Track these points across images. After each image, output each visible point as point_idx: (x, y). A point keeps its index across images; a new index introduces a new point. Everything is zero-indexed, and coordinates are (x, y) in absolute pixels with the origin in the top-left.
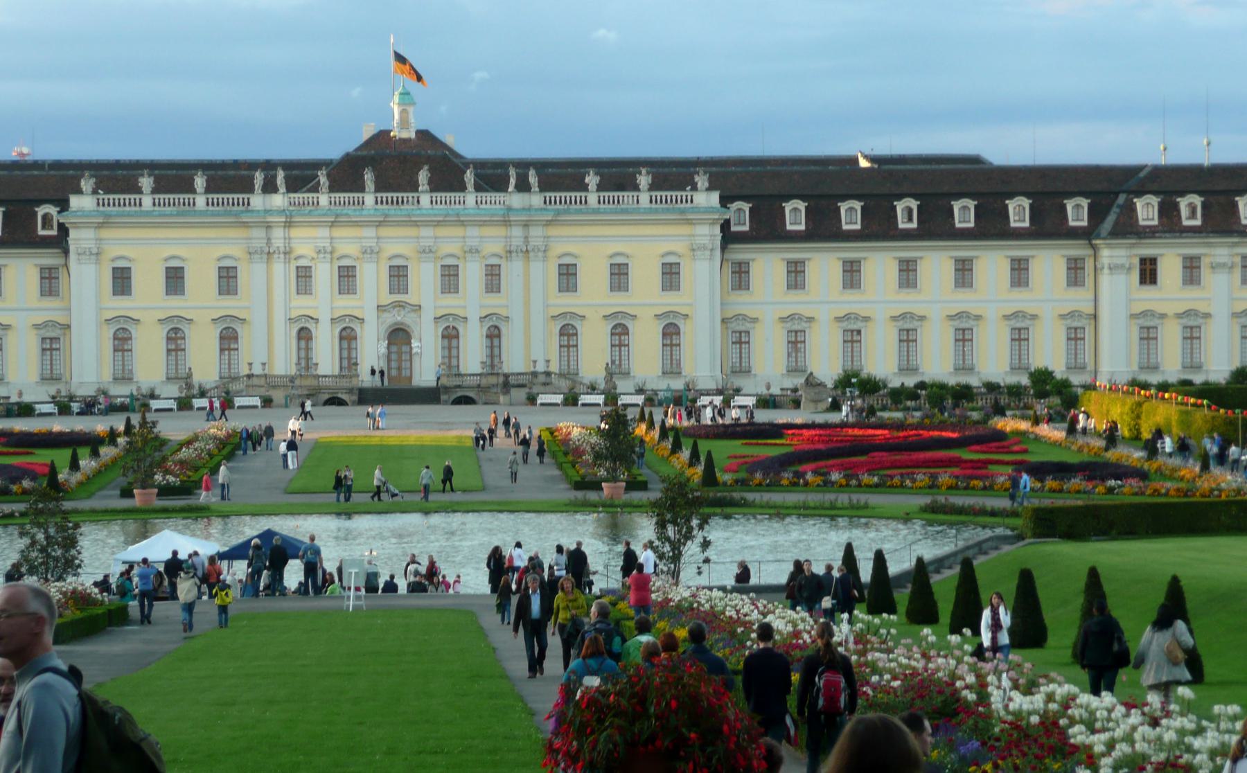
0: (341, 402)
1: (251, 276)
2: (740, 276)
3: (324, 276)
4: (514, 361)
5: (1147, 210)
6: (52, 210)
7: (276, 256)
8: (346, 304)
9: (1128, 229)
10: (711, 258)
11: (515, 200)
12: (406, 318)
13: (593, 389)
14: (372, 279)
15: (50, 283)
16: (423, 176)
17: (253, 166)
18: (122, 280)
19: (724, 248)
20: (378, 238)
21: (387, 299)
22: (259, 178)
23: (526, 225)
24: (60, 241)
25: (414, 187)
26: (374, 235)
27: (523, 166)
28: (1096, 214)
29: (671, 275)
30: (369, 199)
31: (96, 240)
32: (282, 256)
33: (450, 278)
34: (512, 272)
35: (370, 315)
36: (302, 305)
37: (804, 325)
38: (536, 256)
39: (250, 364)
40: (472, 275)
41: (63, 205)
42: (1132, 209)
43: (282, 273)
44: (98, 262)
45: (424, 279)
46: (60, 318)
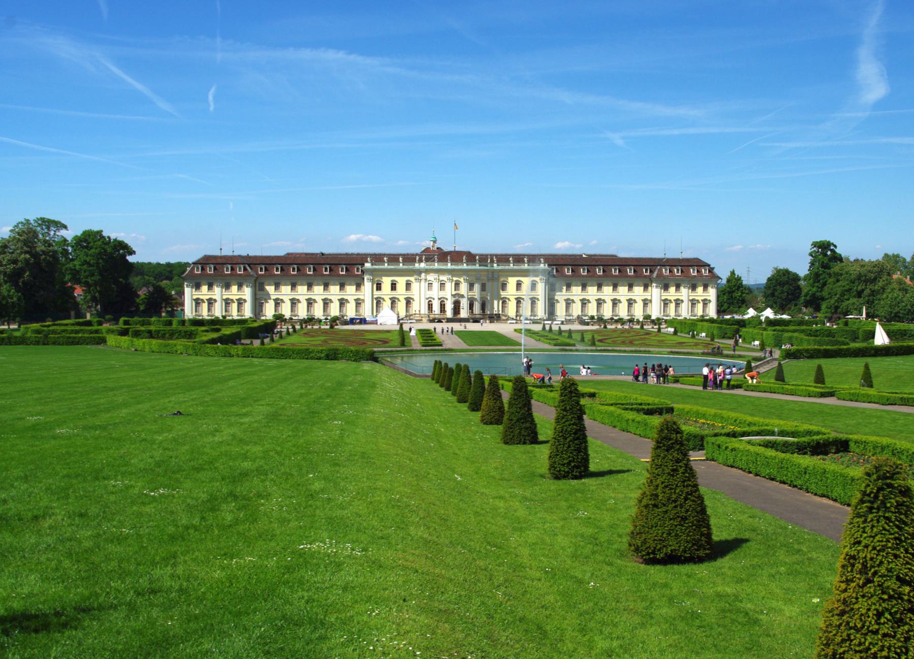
0: (442, 322)
1: (415, 286)
3: (436, 285)
5: (665, 272)
6: (360, 267)
8: (442, 294)
13: (513, 319)
14: (450, 287)
18: (379, 287)
21: (454, 293)
22: (417, 258)
25: (462, 261)
29: (533, 286)
30: (449, 264)
35: (449, 296)
36: (429, 294)
41: (363, 265)
42: (660, 270)
43: (424, 285)
45: (464, 289)
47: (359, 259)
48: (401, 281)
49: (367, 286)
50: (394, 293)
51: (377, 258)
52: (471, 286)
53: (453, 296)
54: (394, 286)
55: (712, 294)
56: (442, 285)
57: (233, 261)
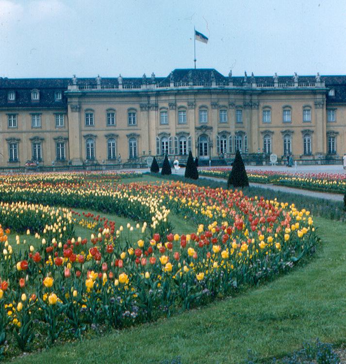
1: (141, 116)
7: (152, 108)
10: (323, 108)
12: (207, 133)
19: (327, 105)
20: (195, 99)
23: (251, 95)
26: (193, 98)
31: (79, 102)
32: (154, 108)
37: (335, 135)
38: (255, 107)
39: (144, 152)
44: (79, 111)
46: (64, 135)
48: (122, 109)
49: (74, 119)
53: (197, 128)
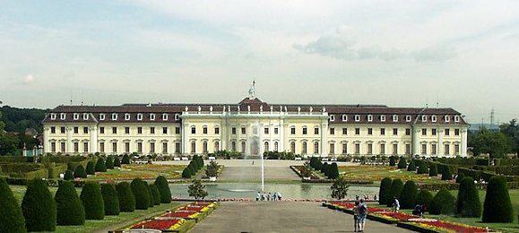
2: (332, 132)
4: (280, 150)
9: (420, 122)
11: (282, 113)
15: (178, 131)
16: (261, 108)
17: (222, 105)
24: (180, 121)
27: (283, 106)
28: (414, 119)
33: (267, 131)
34: (281, 130)
40: (272, 130)
42: (421, 118)
47: (180, 108)
49: (187, 130)
50: (205, 135)
51: (193, 108)
52: (267, 131)
54: (205, 131)
55: (463, 138)
56: (244, 131)
57: (81, 110)
